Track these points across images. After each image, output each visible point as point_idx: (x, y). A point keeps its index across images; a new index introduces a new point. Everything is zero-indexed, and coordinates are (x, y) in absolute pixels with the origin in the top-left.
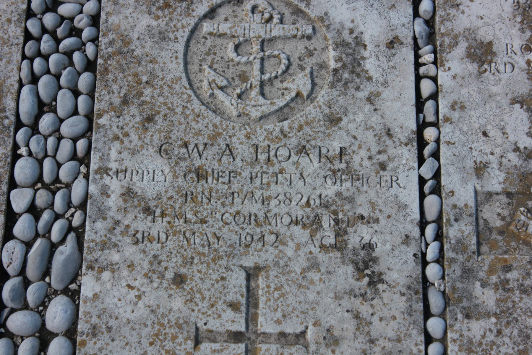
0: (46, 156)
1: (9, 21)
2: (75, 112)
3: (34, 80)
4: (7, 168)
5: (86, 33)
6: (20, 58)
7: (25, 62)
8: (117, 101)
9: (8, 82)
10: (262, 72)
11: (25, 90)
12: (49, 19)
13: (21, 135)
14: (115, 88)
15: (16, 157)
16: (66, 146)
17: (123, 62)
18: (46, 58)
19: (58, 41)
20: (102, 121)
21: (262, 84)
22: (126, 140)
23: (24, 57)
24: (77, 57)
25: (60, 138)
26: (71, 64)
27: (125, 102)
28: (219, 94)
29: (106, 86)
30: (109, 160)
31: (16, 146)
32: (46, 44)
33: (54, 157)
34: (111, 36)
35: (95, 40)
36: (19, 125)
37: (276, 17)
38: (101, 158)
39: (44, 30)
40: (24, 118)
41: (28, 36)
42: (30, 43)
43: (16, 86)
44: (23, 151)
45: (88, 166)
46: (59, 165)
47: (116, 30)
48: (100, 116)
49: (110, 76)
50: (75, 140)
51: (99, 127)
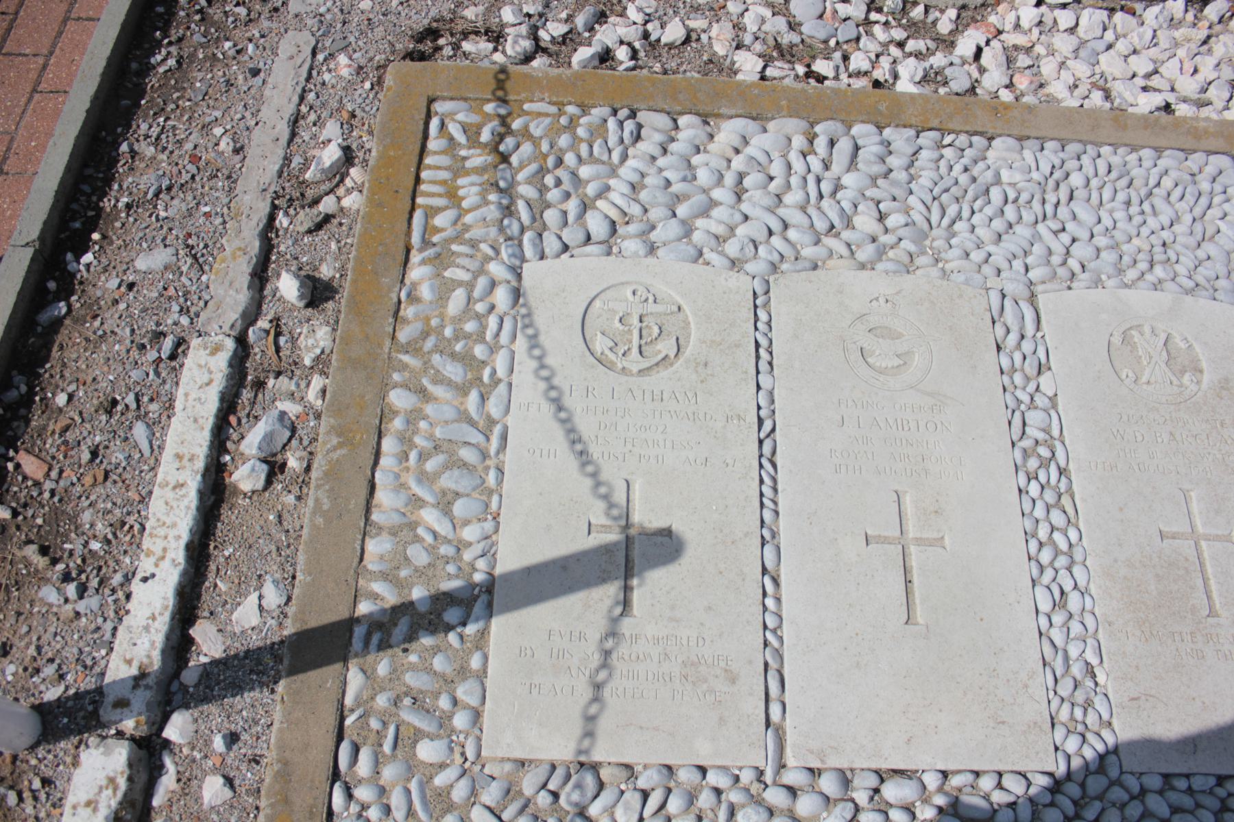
10: (641, 337)
21: (640, 346)
28: (607, 352)
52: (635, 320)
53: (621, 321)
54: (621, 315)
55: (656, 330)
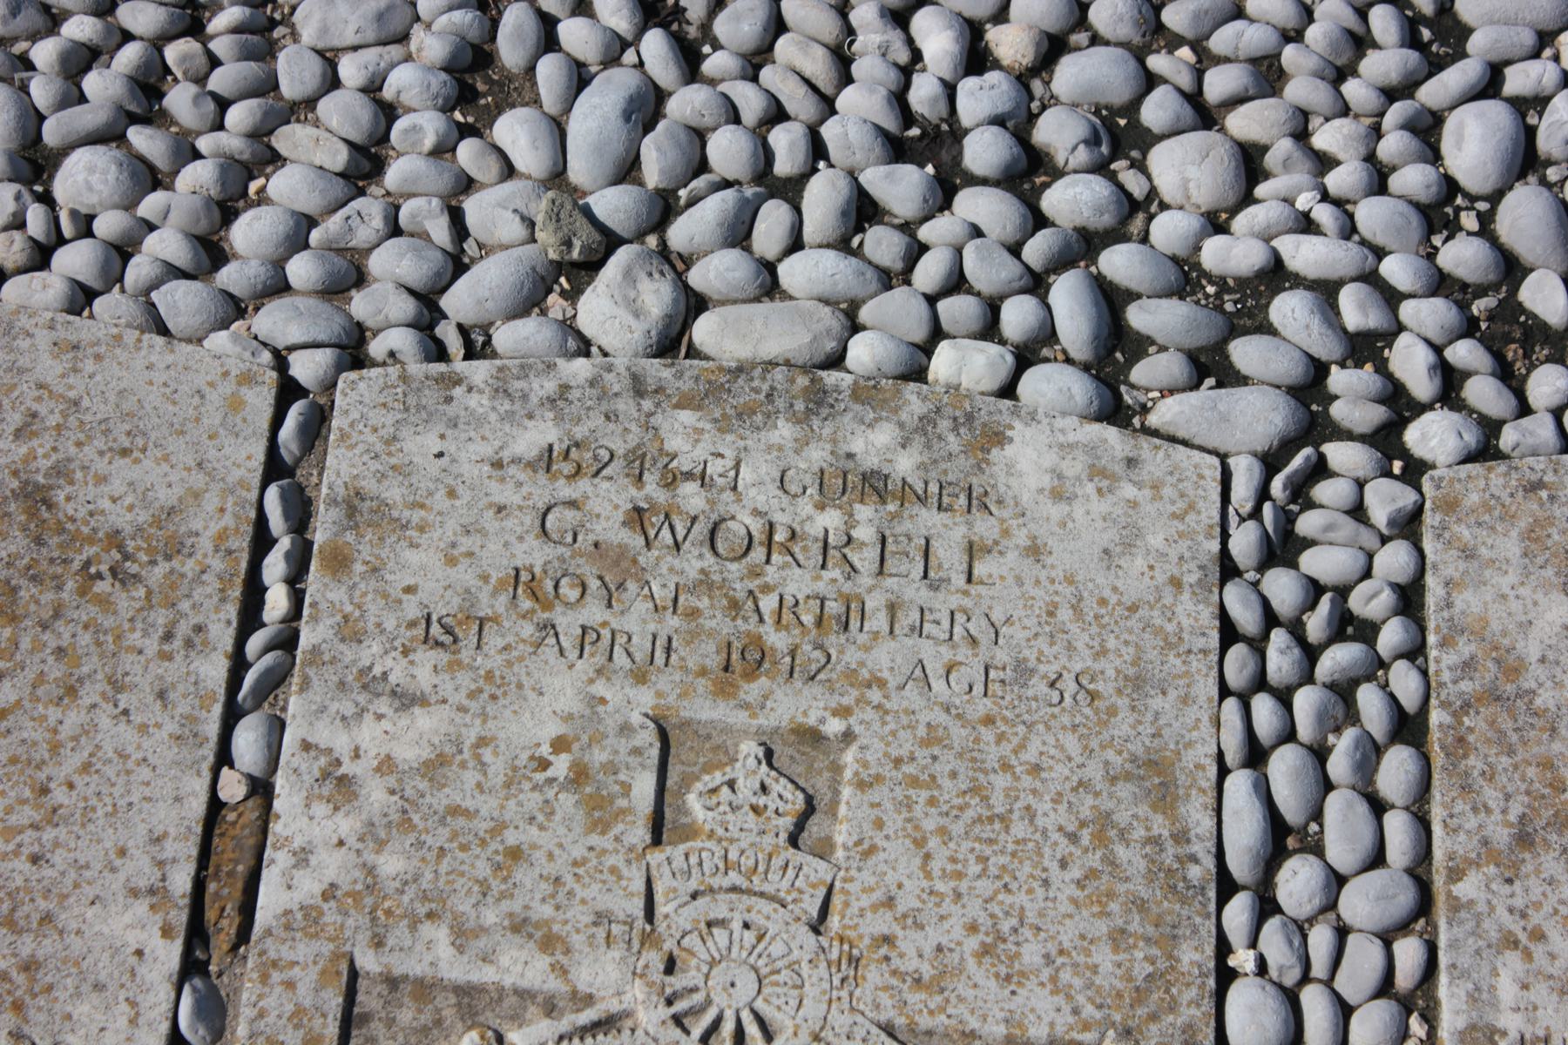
0: (1306, 979)
1: (1176, 583)
2: (1377, 859)
3: (1256, 755)
4: (1208, 1006)
5: (1392, 636)
6: (1215, 692)
7: (1231, 704)
8: (1501, 836)
9: (1189, 758)
11: (1239, 784)
12: (1282, 587)
13: (1238, 911)
14: (1491, 795)
15: (1226, 976)
16: (1363, 960)
17: (1507, 724)
18: (1284, 698)
19: (1311, 653)
20: (1467, 888)
22: (1538, 950)
23: (1224, 691)
24: (1369, 699)
25: (1342, 932)
26: (1352, 715)
27: (1524, 839)
29: (1466, 789)
30: (1494, 1004)
31: (1223, 947)
32: (1280, 658)
33: (1329, 983)
34: (1466, 648)
35: (1415, 653)
36: (1227, 887)
38: (1473, 998)
39: (1271, 619)
40: (1240, 865)
41: (1229, 633)
42: (1237, 652)
43: (1213, 771)
44: (1243, 959)
45: (1430, 1019)
46: (1345, 1011)
47: (1478, 631)
48: (1455, 875)
49: (1474, 762)
50: (1387, 939)
51: (1456, 905)
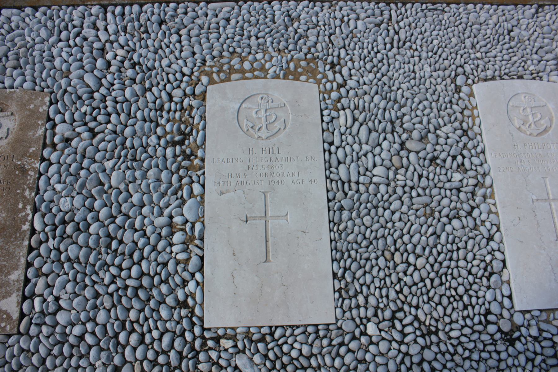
28: (250, 129)
37: (270, 101)
52: (263, 112)
53: (256, 113)
54: (256, 110)
55: (274, 117)
